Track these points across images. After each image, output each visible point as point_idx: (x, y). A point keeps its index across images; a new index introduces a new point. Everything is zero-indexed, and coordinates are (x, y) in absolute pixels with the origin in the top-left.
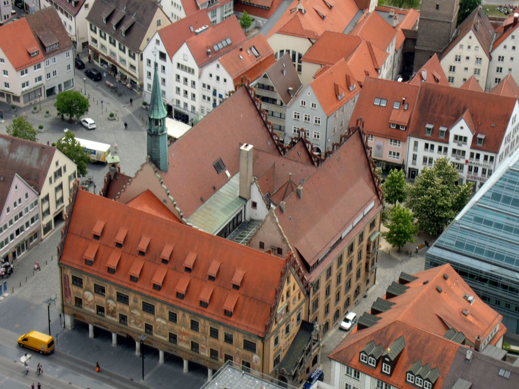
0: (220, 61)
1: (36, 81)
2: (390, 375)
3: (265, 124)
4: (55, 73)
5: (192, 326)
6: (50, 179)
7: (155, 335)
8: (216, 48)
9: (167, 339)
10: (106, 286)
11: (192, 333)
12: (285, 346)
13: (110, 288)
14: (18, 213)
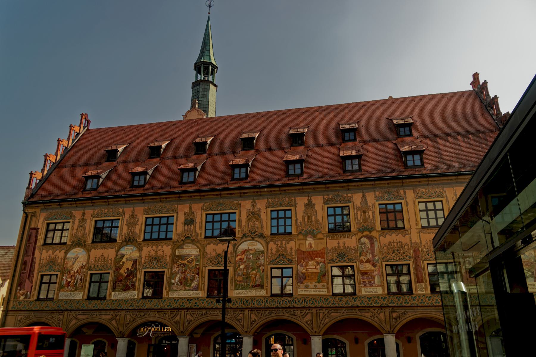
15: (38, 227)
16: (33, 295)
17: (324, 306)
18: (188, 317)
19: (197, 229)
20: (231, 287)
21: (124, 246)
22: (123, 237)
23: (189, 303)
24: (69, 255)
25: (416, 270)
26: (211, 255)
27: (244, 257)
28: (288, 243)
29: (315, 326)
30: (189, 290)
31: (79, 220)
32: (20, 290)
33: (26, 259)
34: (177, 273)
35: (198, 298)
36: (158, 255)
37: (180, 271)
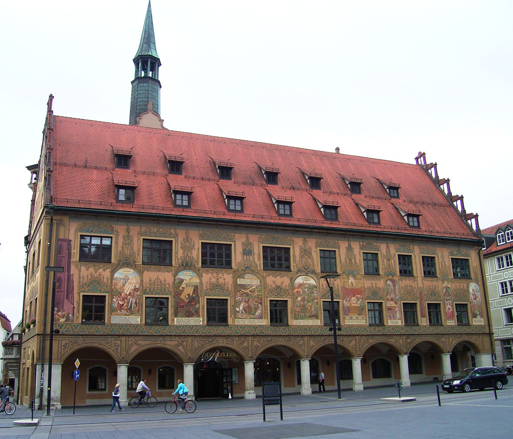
10: (176, 236)
11: (368, 283)
13: (187, 239)
15: (70, 238)
16: (77, 317)
17: (364, 334)
18: (255, 342)
19: (256, 260)
20: (292, 317)
21: (181, 271)
22: (180, 261)
23: (255, 330)
24: (116, 275)
25: (421, 308)
26: (271, 286)
27: (299, 290)
28: (335, 280)
29: (358, 350)
30: (254, 318)
31: (124, 237)
32: (58, 311)
33: (58, 275)
34: (241, 302)
35: (263, 326)
36: (220, 282)
37: (243, 300)
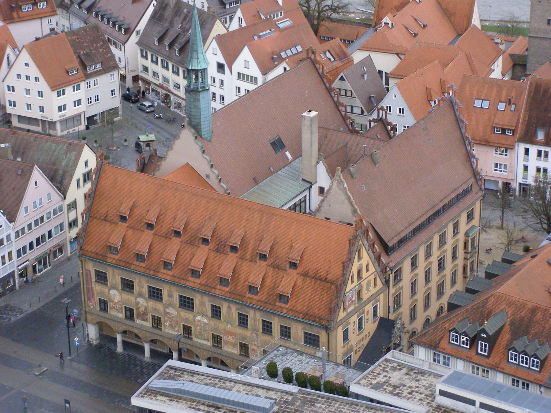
0: (286, 62)
1: (75, 106)
2: (488, 357)
3: (337, 105)
4: (97, 98)
5: (240, 322)
6: (78, 181)
7: (196, 340)
8: (283, 55)
9: (209, 344)
10: (135, 279)
11: (240, 331)
12: (358, 346)
13: (140, 282)
14: (38, 217)
24: (111, 292)
